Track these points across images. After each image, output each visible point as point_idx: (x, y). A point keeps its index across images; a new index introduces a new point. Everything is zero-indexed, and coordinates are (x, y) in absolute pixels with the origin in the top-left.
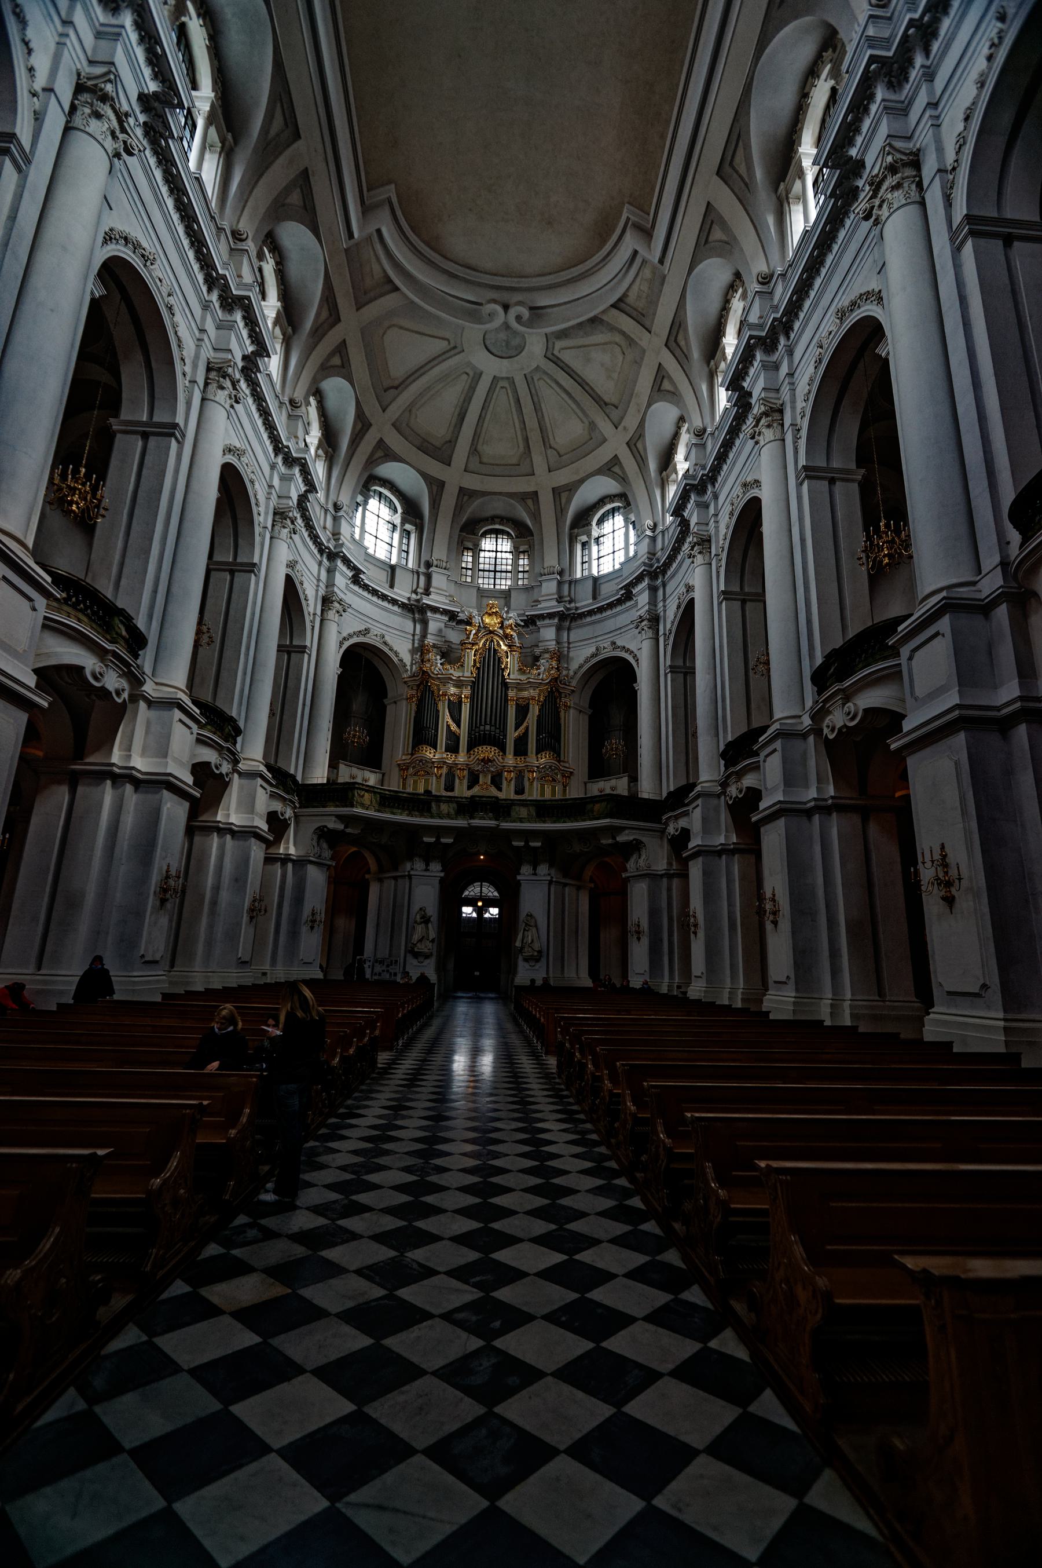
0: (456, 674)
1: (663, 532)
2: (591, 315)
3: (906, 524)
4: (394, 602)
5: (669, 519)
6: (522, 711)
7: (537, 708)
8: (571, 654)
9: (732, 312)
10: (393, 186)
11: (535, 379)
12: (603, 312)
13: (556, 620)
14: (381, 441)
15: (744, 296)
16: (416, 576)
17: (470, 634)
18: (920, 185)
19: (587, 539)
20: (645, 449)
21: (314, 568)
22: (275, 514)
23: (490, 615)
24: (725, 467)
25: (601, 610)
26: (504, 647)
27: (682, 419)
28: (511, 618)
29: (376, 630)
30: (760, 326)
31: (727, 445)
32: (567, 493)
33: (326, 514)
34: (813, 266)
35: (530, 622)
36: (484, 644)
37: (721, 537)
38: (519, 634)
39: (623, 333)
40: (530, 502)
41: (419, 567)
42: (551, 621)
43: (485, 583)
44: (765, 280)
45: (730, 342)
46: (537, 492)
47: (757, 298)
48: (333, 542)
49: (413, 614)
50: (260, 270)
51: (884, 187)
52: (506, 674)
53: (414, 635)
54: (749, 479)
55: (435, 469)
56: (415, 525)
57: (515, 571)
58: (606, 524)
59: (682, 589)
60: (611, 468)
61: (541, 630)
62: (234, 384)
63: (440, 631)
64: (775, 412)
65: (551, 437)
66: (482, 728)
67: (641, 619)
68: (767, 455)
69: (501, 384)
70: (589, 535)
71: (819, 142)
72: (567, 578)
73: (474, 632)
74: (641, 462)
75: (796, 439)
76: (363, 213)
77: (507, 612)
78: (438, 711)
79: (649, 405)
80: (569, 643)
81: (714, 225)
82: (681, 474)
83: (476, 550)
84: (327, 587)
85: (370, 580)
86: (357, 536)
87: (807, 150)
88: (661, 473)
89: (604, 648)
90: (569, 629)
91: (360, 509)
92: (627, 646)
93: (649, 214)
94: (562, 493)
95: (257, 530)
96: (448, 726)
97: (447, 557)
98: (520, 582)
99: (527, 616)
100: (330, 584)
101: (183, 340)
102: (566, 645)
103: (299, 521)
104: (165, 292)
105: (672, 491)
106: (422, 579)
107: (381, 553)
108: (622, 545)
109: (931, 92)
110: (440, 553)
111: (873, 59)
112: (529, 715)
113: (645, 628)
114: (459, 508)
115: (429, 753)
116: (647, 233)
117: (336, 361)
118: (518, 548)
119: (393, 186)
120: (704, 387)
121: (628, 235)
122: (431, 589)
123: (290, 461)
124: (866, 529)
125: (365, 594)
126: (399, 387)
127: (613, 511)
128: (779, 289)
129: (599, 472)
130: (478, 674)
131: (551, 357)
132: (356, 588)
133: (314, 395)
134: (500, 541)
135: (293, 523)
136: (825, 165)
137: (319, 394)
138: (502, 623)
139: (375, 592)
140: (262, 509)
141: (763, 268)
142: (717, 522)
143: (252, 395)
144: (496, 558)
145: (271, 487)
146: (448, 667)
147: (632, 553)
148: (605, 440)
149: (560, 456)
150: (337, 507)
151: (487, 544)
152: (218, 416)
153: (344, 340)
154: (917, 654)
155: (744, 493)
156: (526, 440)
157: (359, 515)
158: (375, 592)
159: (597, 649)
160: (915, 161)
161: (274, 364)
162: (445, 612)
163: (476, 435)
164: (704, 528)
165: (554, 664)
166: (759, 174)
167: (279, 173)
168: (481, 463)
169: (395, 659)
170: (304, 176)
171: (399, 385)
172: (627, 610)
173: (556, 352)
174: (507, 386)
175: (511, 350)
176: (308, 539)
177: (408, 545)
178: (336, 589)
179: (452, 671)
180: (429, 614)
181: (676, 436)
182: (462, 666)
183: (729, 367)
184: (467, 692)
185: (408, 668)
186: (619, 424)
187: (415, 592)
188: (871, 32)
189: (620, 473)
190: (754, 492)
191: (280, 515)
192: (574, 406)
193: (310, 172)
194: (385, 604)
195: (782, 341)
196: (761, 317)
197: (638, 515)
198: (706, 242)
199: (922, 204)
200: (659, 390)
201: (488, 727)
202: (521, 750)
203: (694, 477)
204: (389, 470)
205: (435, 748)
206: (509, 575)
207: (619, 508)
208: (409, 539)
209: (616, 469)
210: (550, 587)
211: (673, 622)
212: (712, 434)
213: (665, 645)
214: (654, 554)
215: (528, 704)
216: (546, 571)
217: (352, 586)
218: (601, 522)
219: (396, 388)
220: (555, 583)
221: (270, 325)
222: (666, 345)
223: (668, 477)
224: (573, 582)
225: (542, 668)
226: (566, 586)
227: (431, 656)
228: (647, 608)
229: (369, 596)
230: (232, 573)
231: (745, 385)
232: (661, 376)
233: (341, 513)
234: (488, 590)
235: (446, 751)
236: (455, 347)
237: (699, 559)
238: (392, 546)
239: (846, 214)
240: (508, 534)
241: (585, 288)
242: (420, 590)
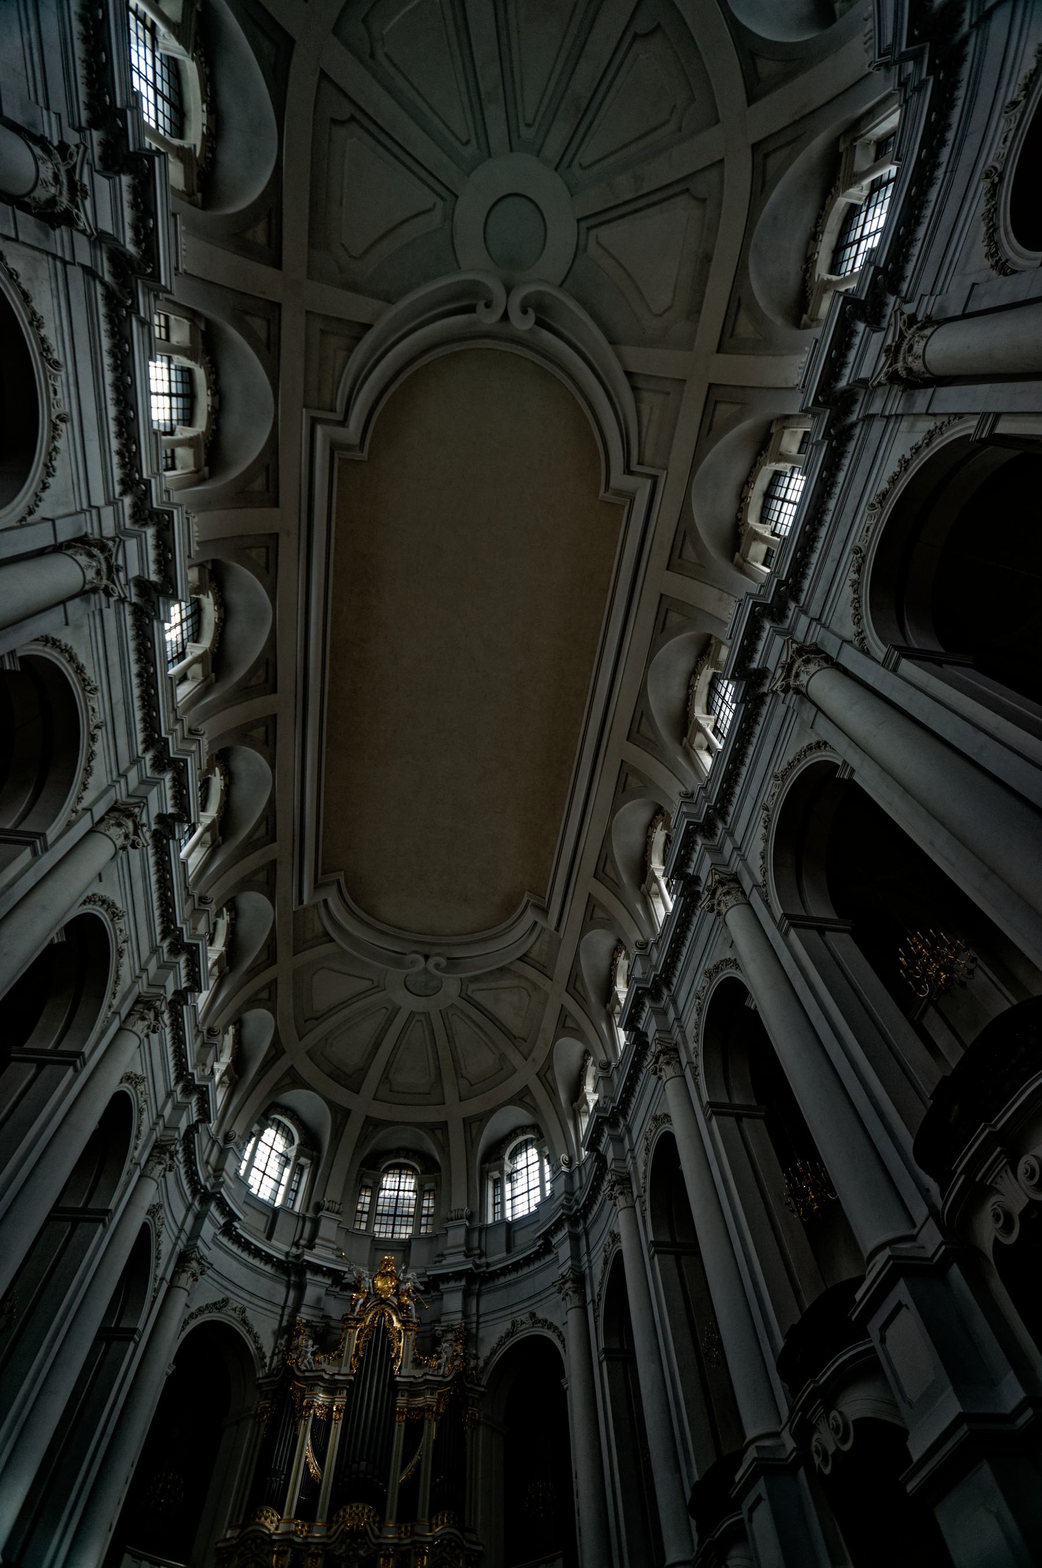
0: (330, 1369)
1: (579, 1168)
2: (501, 965)
3: (822, 1165)
4: (268, 1259)
5: (584, 1153)
6: (414, 1431)
7: (434, 1425)
8: (481, 1334)
9: (619, 968)
10: (343, 873)
11: (450, 1016)
12: (511, 963)
13: (463, 1283)
14: (292, 1067)
15: (627, 957)
16: (301, 1223)
17: (356, 1305)
18: (743, 892)
19: (499, 1175)
20: (554, 1079)
21: (180, 1211)
22: (155, 1147)
23: (384, 1276)
24: (634, 1101)
25: (517, 1266)
26: (396, 1324)
27: (586, 1054)
28: (409, 1279)
29: (236, 1302)
30: (646, 980)
31: (633, 1079)
32: (478, 1123)
33: (213, 1146)
34: (679, 940)
35: (432, 1285)
36: (372, 1321)
37: (641, 1176)
38: (418, 1304)
39: (527, 979)
40: (438, 1132)
41: (307, 1210)
42: (458, 1284)
43: (382, 1231)
44: (643, 946)
45: (622, 990)
47: (638, 959)
48: (212, 1180)
50: (215, 924)
51: (718, 893)
52: (396, 1368)
53: (283, 1308)
54: (658, 1113)
55: (343, 1096)
56: (311, 1158)
57: (418, 1215)
58: (519, 1159)
59: (607, 1239)
60: (522, 1098)
61: (445, 1297)
62: (158, 1015)
63: (319, 1300)
64: (671, 1052)
65: (463, 1067)
66: (355, 1466)
67: (564, 1279)
68: (671, 1089)
69: (417, 1018)
70: (502, 1171)
71: (664, 862)
72: (476, 1224)
73: (361, 1301)
74: (552, 1092)
75: (695, 1077)
76: (315, 888)
77: (405, 1272)
78: (296, 1437)
79: (556, 1038)
80: (479, 1316)
81: (596, 908)
82: (592, 1106)
83: (376, 1188)
84: (189, 1239)
85: (244, 1229)
86: (242, 1173)
87: (657, 867)
88: (572, 1104)
89: (522, 1323)
90: (479, 1296)
91: (254, 1139)
92: (550, 1320)
94: (474, 1124)
95: (128, 1166)
96: (307, 1466)
97: (342, 1197)
98: (423, 1230)
99: (429, 1276)
100: (195, 1234)
101: (122, 978)
102: (475, 1319)
103: (180, 1156)
104: (121, 938)
105: (584, 1123)
106: (308, 1226)
107: (265, 1194)
108: (537, 1183)
109: (734, 842)
110: (334, 1193)
111: (689, 823)
112: (424, 1440)
113: (570, 1293)
114: (362, 1140)
115: (272, 1524)
116: (545, 911)
117: (265, 995)
118: (423, 1186)
119: (343, 873)
120: (604, 1026)
121: (529, 911)
122: (317, 1241)
123: (190, 1088)
124: (785, 1170)
125: (234, 1248)
126: (319, 1018)
127: (525, 1145)
128: (655, 954)
129: (510, 1102)
130: (359, 1369)
131: (465, 996)
132: (224, 1240)
133: (234, 1024)
134: (403, 1176)
135: (171, 1158)
136: (672, 877)
137: (239, 1023)
138: (397, 1287)
139: (246, 1246)
140: (141, 1143)
141: (640, 938)
142: (634, 1158)
143: (172, 1024)
144: (397, 1198)
145: (160, 1116)
146: (321, 1358)
147: (548, 1193)
148: (515, 1071)
149: (471, 1086)
150: (227, 1138)
151: (389, 1181)
152: (130, 1045)
153: (276, 979)
154: (890, 1333)
155: (657, 1127)
156: (438, 1068)
157: (250, 1147)
158: (246, 1246)
159: (513, 1325)
160: (736, 879)
161: (202, 999)
162: (330, 1273)
163: (389, 1064)
164: (620, 1164)
165: (459, 1348)
166: (625, 878)
168: (391, 1091)
169: (252, 1348)
170: (273, 864)
171: (322, 1016)
172: (547, 1266)
173: (469, 993)
174: (423, 1019)
176: (183, 1177)
177: (299, 1183)
178: (199, 1243)
179: (324, 1366)
180: (309, 1276)
181: (583, 1069)
182: (340, 1356)
183: (623, 1010)
184: (340, 1401)
185: (267, 1360)
186: (529, 1055)
187: (296, 1244)
188: (684, 809)
189: (532, 1104)
190: (665, 1127)
191: (160, 1148)
192: (484, 1038)
193: (278, 861)
194: (256, 1262)
195: (665, 992)
196: (644, 973)
197: (552, 1149)
198: (591, 918)
199: (749, 904)
200: (563, 1027)
201: (363, 1465)
203: (605, 1110)
204: (295, 1097)
205: (281, 1512)
206: (411, 1219)
207: (532, 1140)
208: (301, 1176)
209: (527, 1099)
210: (457, 1236)
211: (601, 1284)
212: (617, 1068)
213: (595, 1318)
214: (572, 1194)
215: (423, 1419)
216: (453, 1214)
217: (220, 1237)
218: (513, 1156)
219: (317, 1019)
220: (462, 1231)
221: (210, 965)
222: (566, 990)
223: (580, 1108)
224: (484, 1229)
225: (444, 1356)
226: (476, 1235)
227: (301, 1340)
228: (569, 1263)
229: (239, 1252)
230: (75, 1223)
231: (640, 1026)
232: (564, 1014)
233: (232, 1145)
234: (384, 1241)
235: (297, 1517)
236: (378, 986)
237: (621, 1201)
238: (279, 1183)
239: (695, 906)
240: (413, 1169)
241: (494, 946)
242: (303, 1242)
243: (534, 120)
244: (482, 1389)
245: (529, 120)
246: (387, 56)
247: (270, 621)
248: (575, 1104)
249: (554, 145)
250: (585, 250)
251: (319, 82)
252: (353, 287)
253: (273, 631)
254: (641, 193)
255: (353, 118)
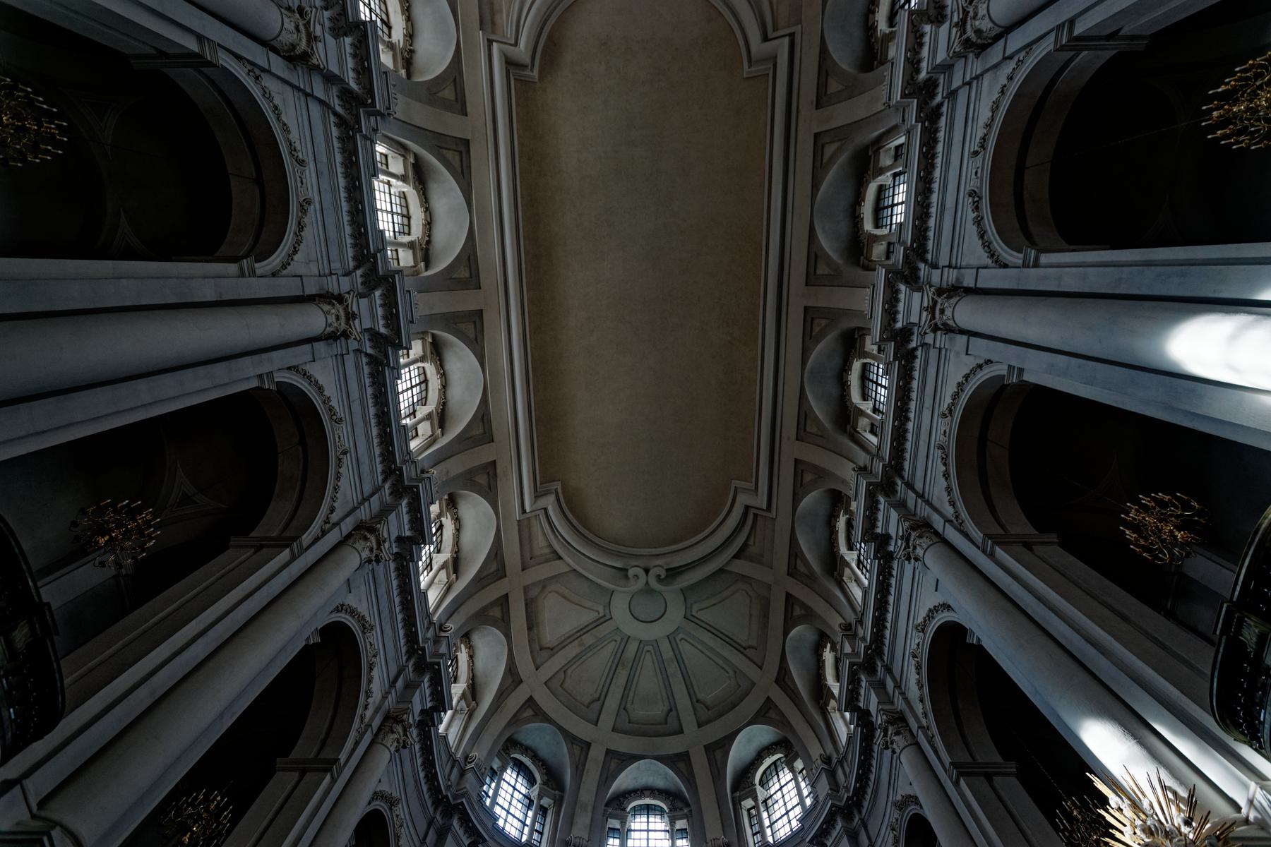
76: (776, 57)
93: (515, 79)
167: (841, 114)
243: (645, 654)
245: (648, 654)
246: (728, 672)
247: (806, 371)
249: (632, 648)
250: (604, 607)
251: (763, 664)
252: (745, 579)
253: (804, 363)
254: (579, 639)
255: (745, 649)
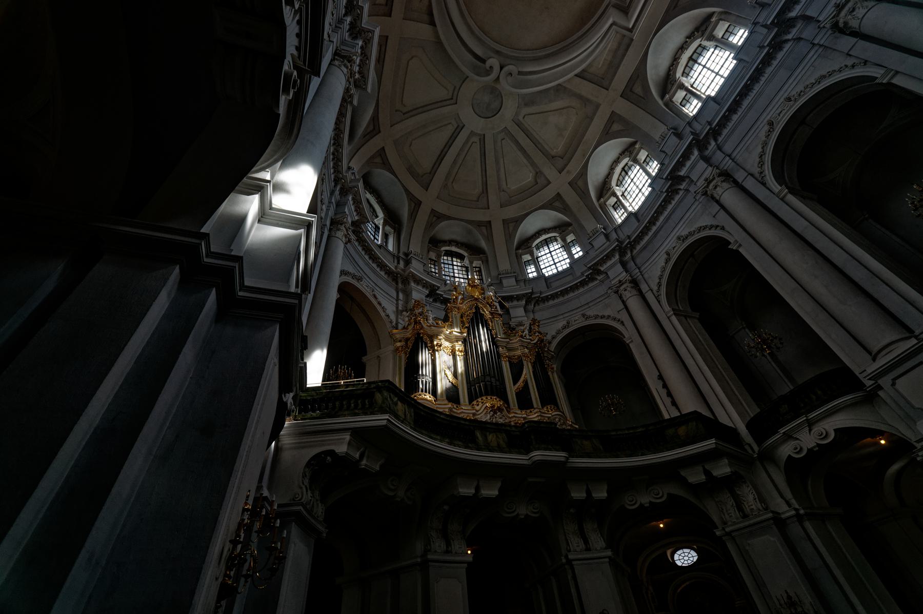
13: (524, 302)
46: (490, 221)
49: (397, 284)
58: (541, 249)
148: (549, 183)
159: (568, 323)
169: (383, 314)
173: (521, 118)
175: (489, 113)
202: (524, 401)
244: (553, 354)
248: (602, 200)
